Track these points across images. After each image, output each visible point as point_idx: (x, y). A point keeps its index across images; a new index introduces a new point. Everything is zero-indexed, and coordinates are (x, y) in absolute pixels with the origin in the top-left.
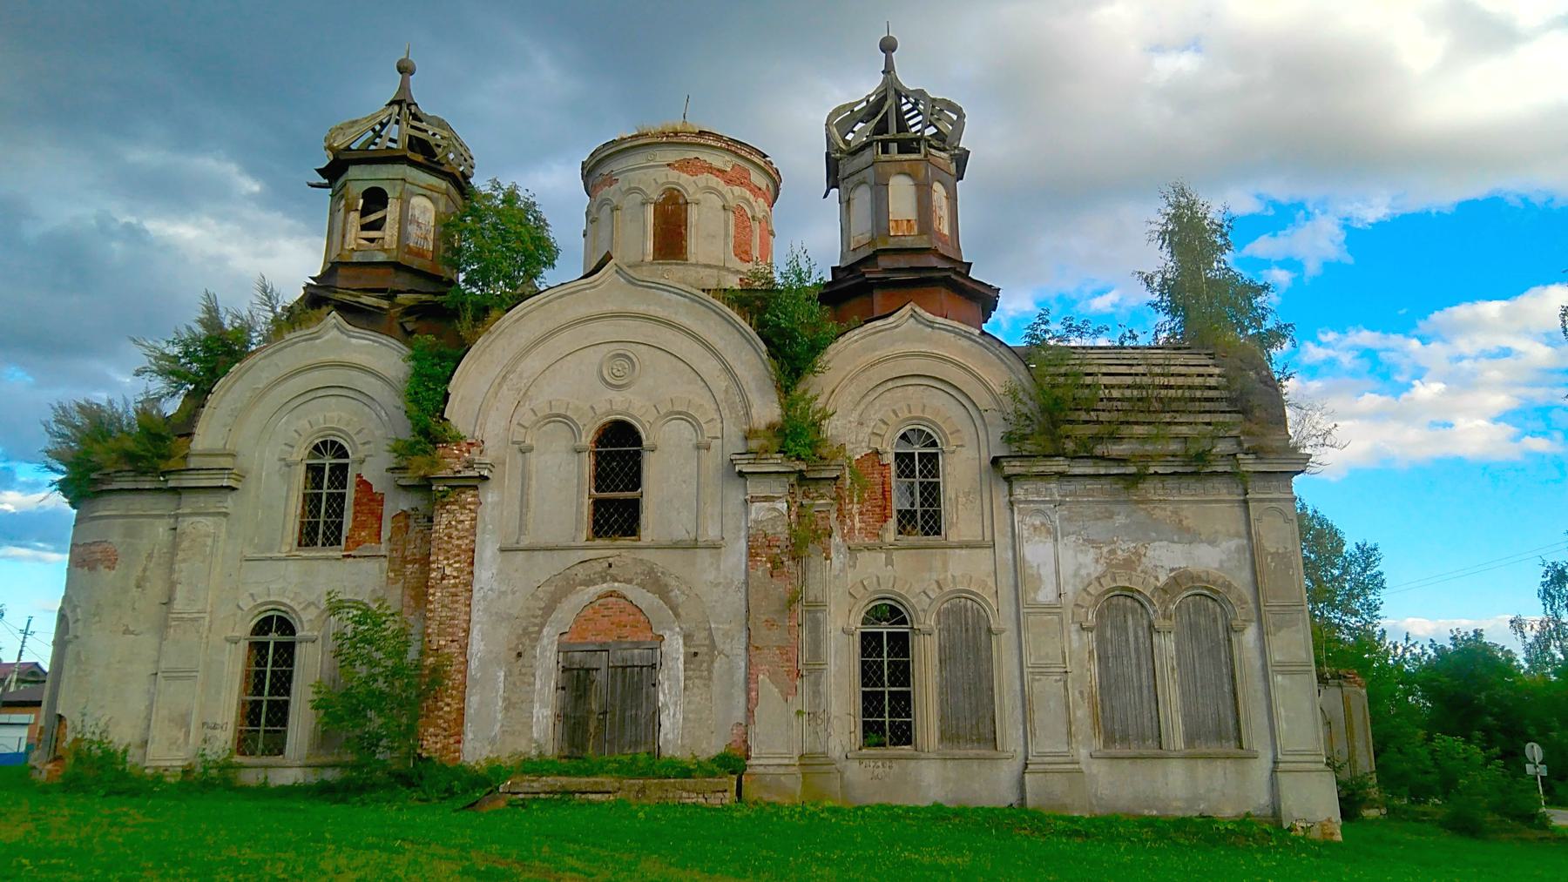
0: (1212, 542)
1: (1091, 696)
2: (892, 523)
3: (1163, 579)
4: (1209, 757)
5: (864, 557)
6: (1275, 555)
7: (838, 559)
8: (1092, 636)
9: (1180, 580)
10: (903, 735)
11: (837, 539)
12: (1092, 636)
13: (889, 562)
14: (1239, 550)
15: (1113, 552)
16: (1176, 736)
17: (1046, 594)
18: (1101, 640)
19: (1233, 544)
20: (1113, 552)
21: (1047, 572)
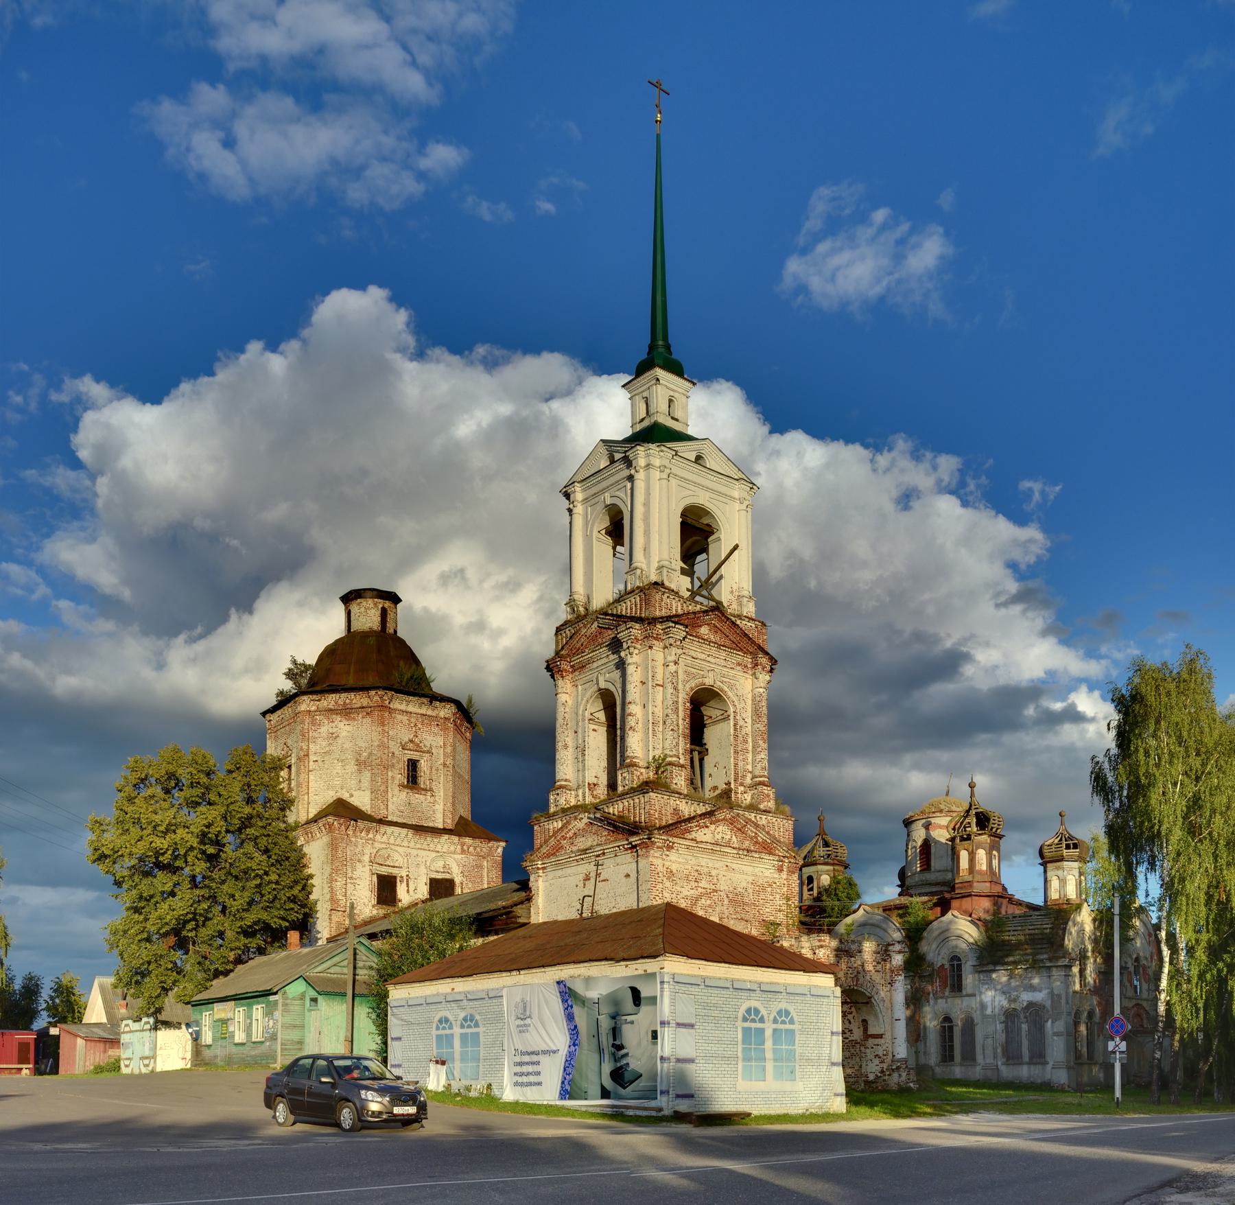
0: (1040, 991)
1: (1002, 1045)
2: (948, 989)
3: (1025, 1004)
4: (1035, 1064)
5: (940, 1001)
6: (1057, 995)
7: (932, 1002)
8: (1003, 1025)
9: (1031, 1005)
10: (952, 1058)
11: (931, 995)
12: (1003, 1025)
13: (946, 1002)
14: (1048, 993)
15: (1010, 996)
16: (1026, 1058)
17: (989, 1012)
18: (1006, 1027)
19: (1047, 991)
20: (1010, 996)
21: (989, 1004)
